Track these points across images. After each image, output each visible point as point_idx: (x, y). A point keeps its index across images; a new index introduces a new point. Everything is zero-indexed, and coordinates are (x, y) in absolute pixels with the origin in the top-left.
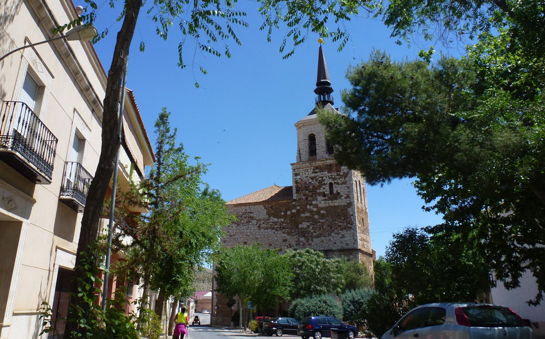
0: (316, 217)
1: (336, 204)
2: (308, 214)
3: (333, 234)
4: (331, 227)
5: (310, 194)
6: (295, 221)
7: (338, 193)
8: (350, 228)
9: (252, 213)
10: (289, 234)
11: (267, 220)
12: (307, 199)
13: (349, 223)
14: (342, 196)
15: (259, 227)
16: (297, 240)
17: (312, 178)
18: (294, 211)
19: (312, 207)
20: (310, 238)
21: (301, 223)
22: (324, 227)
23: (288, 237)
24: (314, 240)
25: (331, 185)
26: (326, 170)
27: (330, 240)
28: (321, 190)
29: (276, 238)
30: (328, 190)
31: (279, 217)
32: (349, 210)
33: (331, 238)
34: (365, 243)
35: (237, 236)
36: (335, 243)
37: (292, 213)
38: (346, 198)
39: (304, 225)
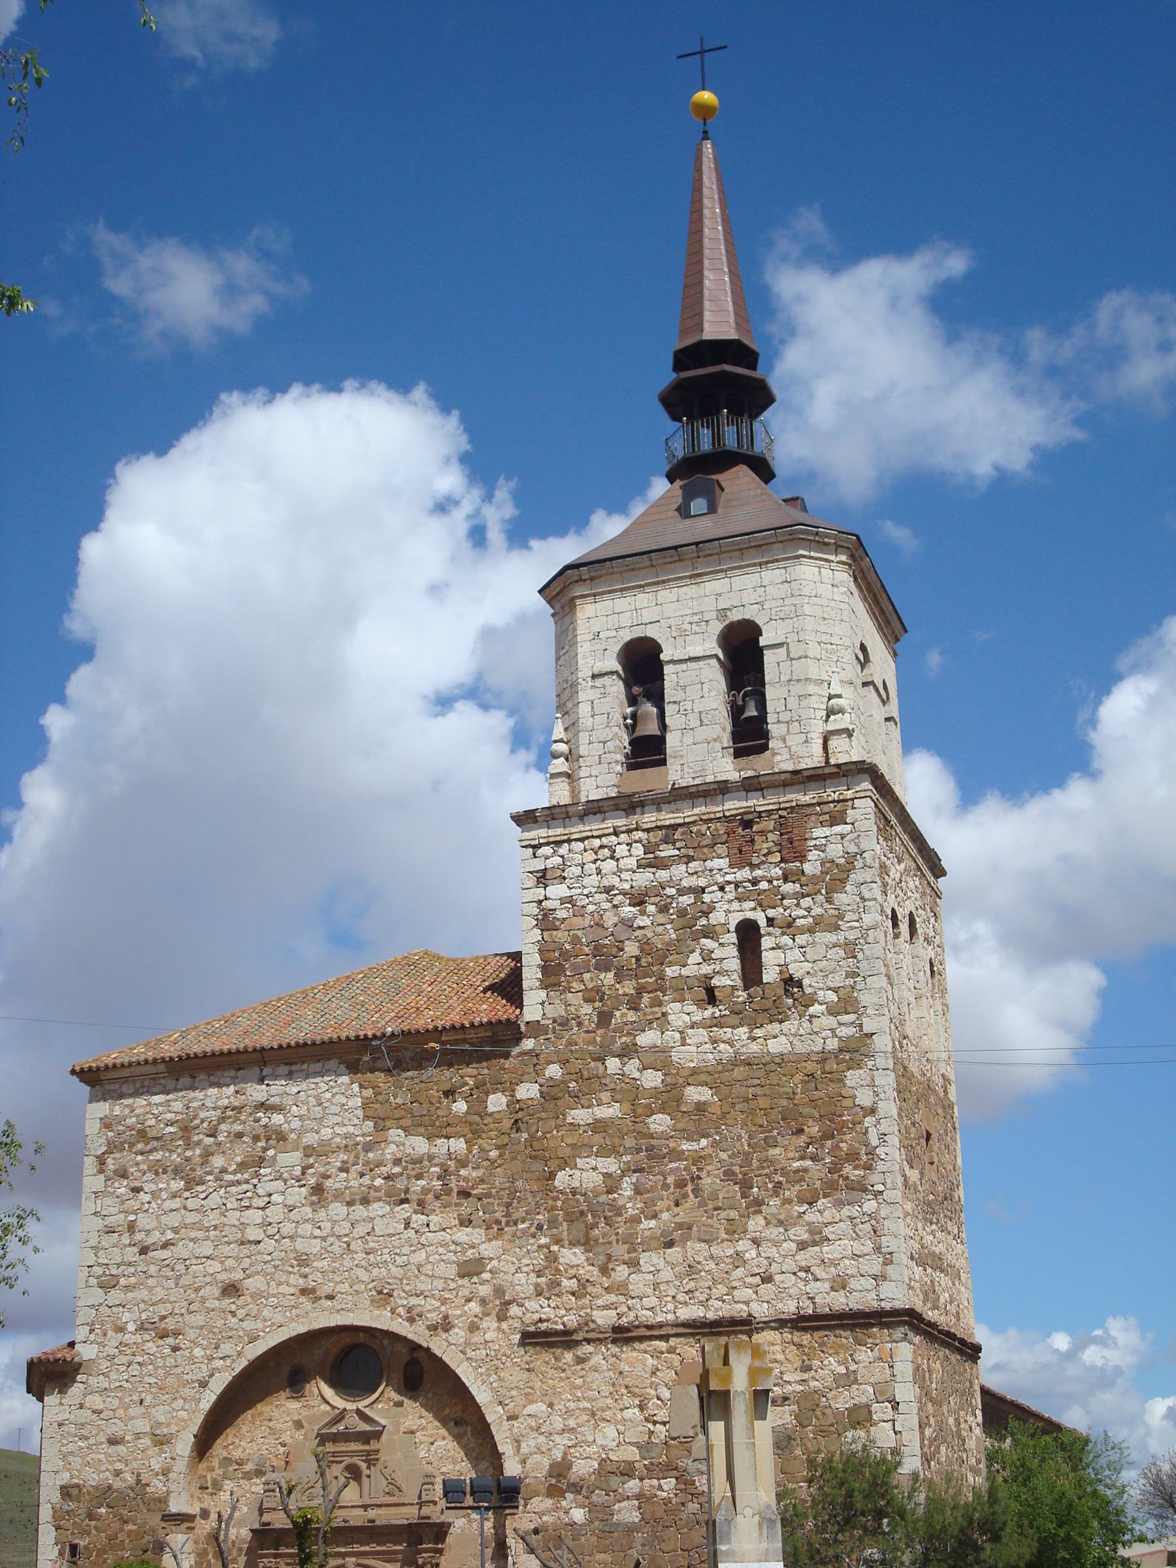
0: (660, 1122)
1: (777, 1046)
2: (610, 1111)
3: (756, 1224)
4: (746, 1185)
5: (628, 987)
6: (533, 1146)
7: (790, 982)
8: (861, 1188)
9: (278, 1109)
10: (494, 1228)
11: (368, 1148)
12: (604, 1018)
13: (852, 1157)
14: (812, 1000)
15: (318, 1189)
16: (540, 1260)
17: (639, 900)
18: (528, 1091)
19: (632, 1067)
20: (620, 1250)
21: (566, 1163)
22: (706, 1181)
23: (488, 1249)
24: (644, 1258)
25: (748, 935)
26: (721, 849)
27: (739, 1259)
28: (694, 966)
29: (421, 1256)
30: (734, 964)
31: (437, 1129)
32: (853, 1077)
33: (743, 1245)
34: (943, 1280)
35: (181, 1250)
36: (767, 1279)
37: (516, 1106)
38: (833, 1011)
39: (585, 1174)
